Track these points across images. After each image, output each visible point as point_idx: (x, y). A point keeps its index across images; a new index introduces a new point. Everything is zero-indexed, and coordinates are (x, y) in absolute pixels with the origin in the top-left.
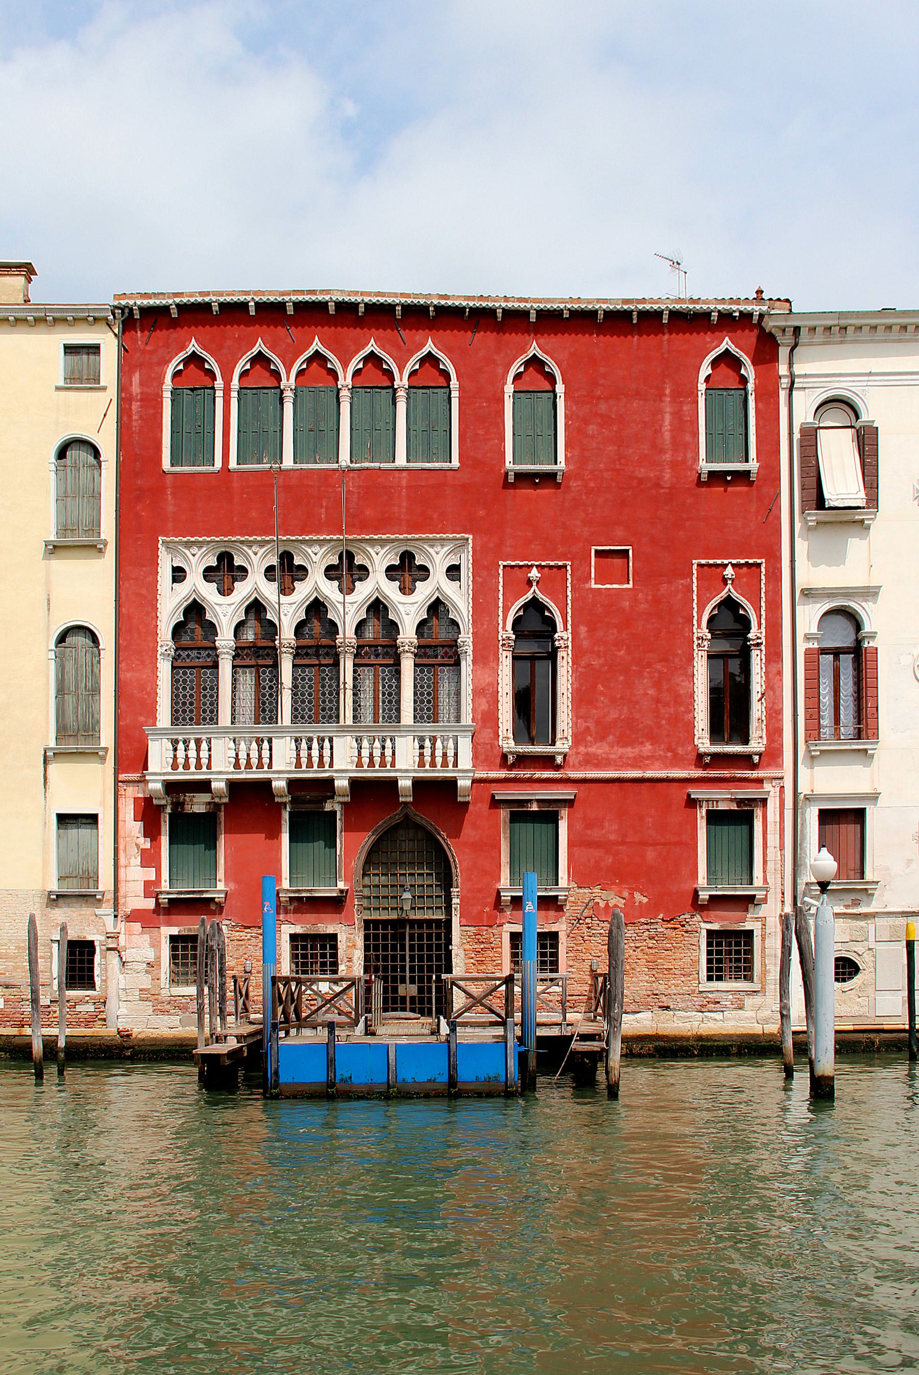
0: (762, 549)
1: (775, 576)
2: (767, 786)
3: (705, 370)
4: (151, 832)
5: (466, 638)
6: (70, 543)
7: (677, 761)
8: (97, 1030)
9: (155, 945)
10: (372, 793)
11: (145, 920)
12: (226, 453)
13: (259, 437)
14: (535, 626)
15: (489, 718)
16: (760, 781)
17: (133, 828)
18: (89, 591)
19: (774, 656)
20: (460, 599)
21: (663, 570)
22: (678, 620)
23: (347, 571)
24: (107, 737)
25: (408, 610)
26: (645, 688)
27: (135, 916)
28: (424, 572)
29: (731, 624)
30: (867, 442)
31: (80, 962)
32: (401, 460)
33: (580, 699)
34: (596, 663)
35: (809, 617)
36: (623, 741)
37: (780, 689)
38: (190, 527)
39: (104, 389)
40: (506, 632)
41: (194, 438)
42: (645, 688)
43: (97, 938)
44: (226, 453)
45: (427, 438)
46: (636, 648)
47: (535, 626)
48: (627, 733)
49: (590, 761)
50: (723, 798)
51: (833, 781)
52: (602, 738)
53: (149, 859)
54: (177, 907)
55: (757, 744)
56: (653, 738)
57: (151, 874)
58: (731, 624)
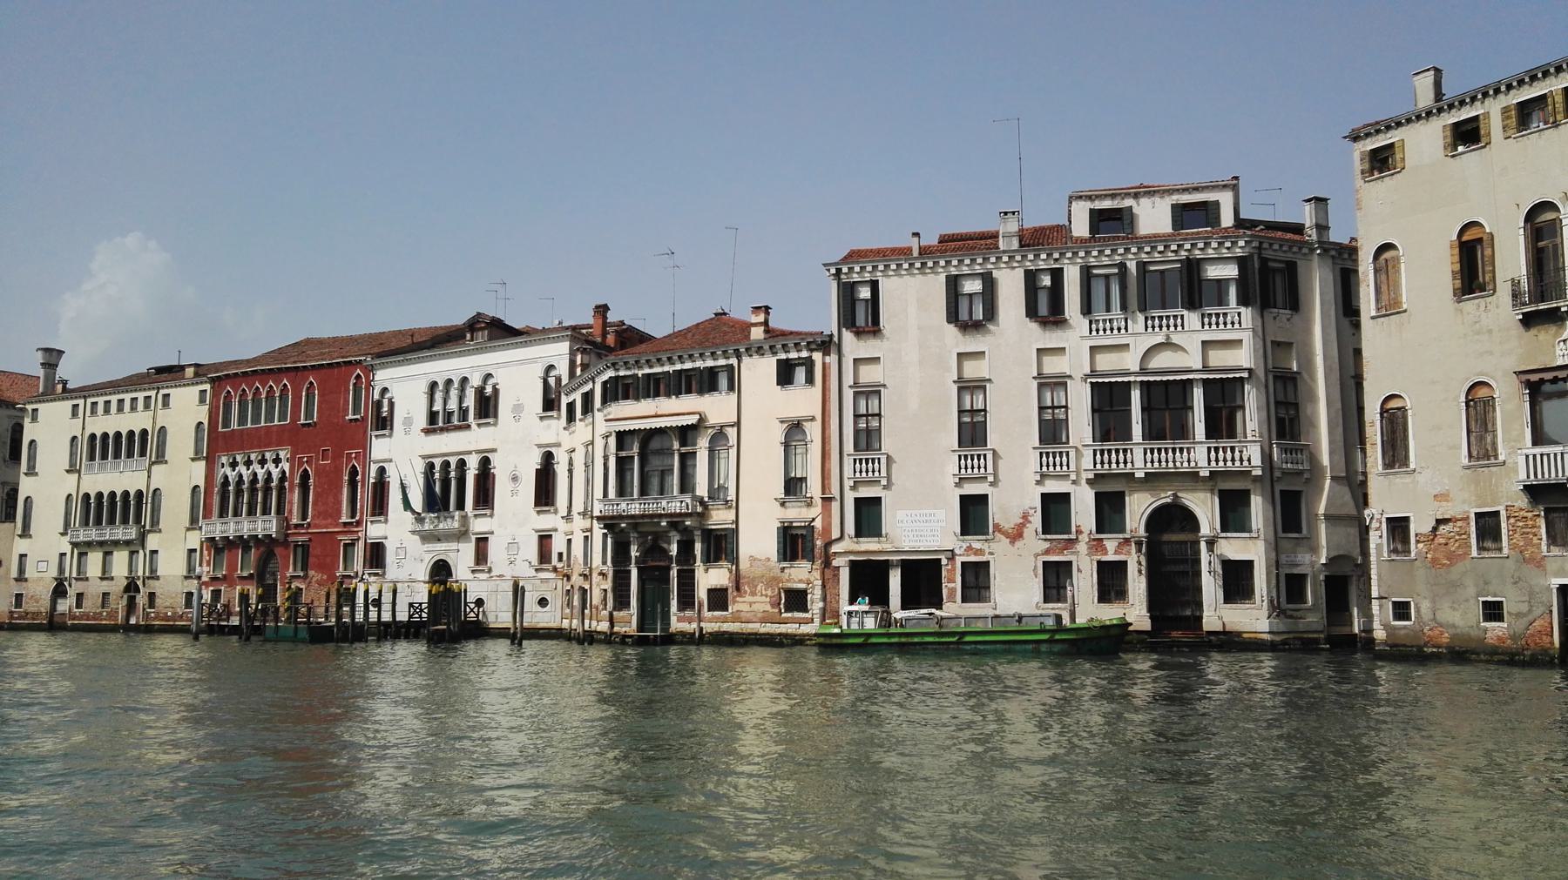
3: (353, 381)
12: (234, 425)
13: (242, 420)
15: (290, 511)
20: (286, 466)
21: (337, 456)
25: (275, 473)
26: (331, 499)
29: (354, 472)
30: (391, 404)
33: (315, 503)
35: (374, 468)
41: (226, 423)
44: (234, 425)
45: (283, 417)
49: (316, 526)
50: (346, 539)
51: (375, 531)
58: (354, 472)
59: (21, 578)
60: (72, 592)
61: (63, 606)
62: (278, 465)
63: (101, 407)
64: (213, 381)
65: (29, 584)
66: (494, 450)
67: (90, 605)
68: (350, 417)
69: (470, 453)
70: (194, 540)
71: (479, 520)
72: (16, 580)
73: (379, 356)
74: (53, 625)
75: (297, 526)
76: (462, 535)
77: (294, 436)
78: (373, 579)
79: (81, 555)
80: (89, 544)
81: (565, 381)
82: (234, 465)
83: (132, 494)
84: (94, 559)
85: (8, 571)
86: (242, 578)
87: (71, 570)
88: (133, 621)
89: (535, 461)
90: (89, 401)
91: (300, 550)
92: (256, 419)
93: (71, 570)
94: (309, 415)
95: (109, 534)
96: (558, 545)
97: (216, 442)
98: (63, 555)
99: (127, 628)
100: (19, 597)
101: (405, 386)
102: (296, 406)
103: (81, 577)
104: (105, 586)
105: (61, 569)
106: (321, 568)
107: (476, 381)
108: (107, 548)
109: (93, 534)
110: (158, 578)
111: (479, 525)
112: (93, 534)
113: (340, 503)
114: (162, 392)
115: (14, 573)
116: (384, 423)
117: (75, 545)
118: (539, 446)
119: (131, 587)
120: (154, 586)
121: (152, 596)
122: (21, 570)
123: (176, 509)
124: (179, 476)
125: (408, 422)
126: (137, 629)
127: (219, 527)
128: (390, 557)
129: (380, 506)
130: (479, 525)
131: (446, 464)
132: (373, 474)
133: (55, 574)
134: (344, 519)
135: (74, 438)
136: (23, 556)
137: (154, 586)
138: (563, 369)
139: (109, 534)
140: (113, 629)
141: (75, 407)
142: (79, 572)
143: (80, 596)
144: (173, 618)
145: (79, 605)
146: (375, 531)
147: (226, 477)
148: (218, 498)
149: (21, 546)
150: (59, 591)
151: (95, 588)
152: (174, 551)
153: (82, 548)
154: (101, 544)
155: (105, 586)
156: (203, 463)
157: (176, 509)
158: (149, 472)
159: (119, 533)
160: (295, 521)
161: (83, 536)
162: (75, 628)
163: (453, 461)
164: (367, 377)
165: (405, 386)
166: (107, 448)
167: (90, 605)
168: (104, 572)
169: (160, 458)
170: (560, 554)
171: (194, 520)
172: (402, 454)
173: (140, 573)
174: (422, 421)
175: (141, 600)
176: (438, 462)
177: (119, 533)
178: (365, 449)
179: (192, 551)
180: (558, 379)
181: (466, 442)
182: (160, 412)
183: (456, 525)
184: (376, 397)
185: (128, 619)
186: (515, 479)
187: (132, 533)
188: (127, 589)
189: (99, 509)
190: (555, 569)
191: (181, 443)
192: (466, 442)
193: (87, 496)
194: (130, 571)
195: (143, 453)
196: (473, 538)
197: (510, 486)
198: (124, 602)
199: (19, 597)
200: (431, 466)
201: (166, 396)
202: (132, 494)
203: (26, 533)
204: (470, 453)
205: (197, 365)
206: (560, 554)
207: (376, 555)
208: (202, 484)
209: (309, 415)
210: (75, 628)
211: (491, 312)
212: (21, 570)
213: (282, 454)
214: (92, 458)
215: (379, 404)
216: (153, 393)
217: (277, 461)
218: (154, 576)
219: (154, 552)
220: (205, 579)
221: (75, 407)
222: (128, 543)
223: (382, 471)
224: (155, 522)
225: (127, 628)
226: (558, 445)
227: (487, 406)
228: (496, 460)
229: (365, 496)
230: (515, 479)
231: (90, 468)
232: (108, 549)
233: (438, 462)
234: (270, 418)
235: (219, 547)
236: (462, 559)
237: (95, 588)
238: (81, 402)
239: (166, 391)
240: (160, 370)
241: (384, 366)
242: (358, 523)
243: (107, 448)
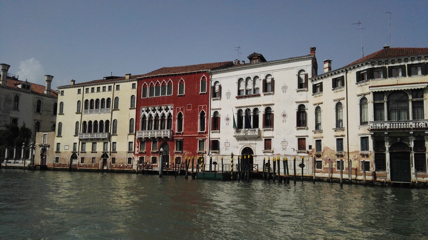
0: (207, 103)
1: (208, 107)
2: (206, 137)
3: (201, 79)
4: (138, 144)
5: (172, 118)
6: (132, 108)
7: (196, 134)
10: (160, 138)
11: (137, 155)
13: (151, 94)
14: (180, 115)
15: (174, 128)
16: (205, 136)
17: (136, 143)
18: (133, 114)
19: (208, 119)
20: (172, 112)
21: (195, 107)
22: (196, 114)
23: (160, 110)
24: (134, 133)
25: (166, 114)
26: (192, 124)
27: (136, 155)
28: (169, 109)
30: (220, 87)
31: (130, 159)
32: (166, 95)
34: (187, 120)
35: (212, 112)
36: (190, 131)
37: (209, 123)
38: (144, 105)
40: (177, 117)
41: (144, 95)
42: (192, 124)
43: (132, 157)
44: (148, 96)
45: (169, 92)
46: (192, 118)
47: (180, 115)
48: (190, 130)
50: (200, 139)
51: (214, 136)
52: (187, 131)
53: (138, 147)
54: (140, 153)
55: (205, 131)
56: (193, 130)
57: (138, 149)
58: (203, 114)
59: (58, 151)
60: (79, 157)
61: (75, 162)
62: (169, 111)
63: (90, 90)
64: (138, 80)
65: (61, 154)
66: (273, 104)
67: (86, 162)
68: (200, 92)
69: (260, 105)
70: (132, 138)
71: (266, 132)
72: (56, 152)
73: (213, 69)
74: (71, 169)
75: (177, 134)
76: (258, 138)
77: (175, 100)
78: (213, 154)
79: (82, 143)
80: (87, 140)
81: (310, 76)
82: (148, 111)
84: (89, 146)
85: (53, 149)
86: (153, 153)
87: (78, 148)
88: (105, 168)
89: (295, 108)
90: (85, 88)
91: (178, 143)
92: (157, 94)
93: (78, 148)
94: (181, 92)
95: (95, 136)
96: (310, 142)
97: (139, 102)
98: (75, 144)
99: (102, 171)
100: (57, 159)
101: (227, 81)
102: (175, 89)
103: (83, 151)
104: (93, 155)
105: (74, 149)
106: (188, 150)
107: (262, 77)
108: (94, 141)
109: (89, 136)
110: (116, 152)
111: (266, 134)
112: (89, 136)
113: (197, 125)
114: (116, 84)
115: (55, 150)
116: (217, 95)
117: (80, 140)
118: (297, 102)
119: (105, 156)
120: (114, 155)
121: (114, 159)
122: (58, 149)
123: (123, 127)
124: (125, 115)
125: (228, 94)
126: (107, 171)
127: (144, 134)
128: (222, 146)
130: (266, 134)
131: (248, 110)
132: (212, 114)
133: (72, 150)
134: (199, 131)
135: (79, 102)
136: (58, 144)
138: (309, 71)
139: (95, 136)
140: (97, 171)
141: (79, 90)
142: (82, 150)
143: (83, 159)
144: (123, 167)
145: (82, 162)
147: (144, 115)
148: (139, 124)
149: (58, 140)
150: (74, 156)
151: (89, 155)
152: (123, 143)
153: (83, 142)
154: (92, 140)
155: (93, 155)
156: (135, 111)
157: (123, 127)
158: (112, 114)
159: (101, 136)
160: (176, 132)
161: (84, 136)
162: (81, 171)
163: (252, 109)
164: (208, 78)
165: (227, 81)
166: (92, 105)
167: (86, 162)
168: (93, 150)
169: (116, 108)
170: (310, 147)
171: (131, 131)
172: (227, 107)
173: (109, 150)
174: (235, 93)
175: (109, 160)
176: (244, 110)
177: (101, 136)
178: (208, 105)
179: (130, 143)
180: (306, 76)
181: (261, 101)
182: (115, 92)
183: (257, 134)
184: (213, 85)
185: (103, 167)
186: (284, 116)
187: (106, 136)
188: (103, 156)
189: (89, 127)
190: (308, 152)
191: (125, 102)
192: (261, 101)
193: (85, 122)
194: (104, 150)
195: (108, 106)
196: (263, 139)
197: (282, 118)
198: (102, 161)
199: (57, 159)
200: (240, 112)
201: (118, 86)
203: (59, 135)
204: (260, 105)
205: (130, 74)
206: (310, 147)
207: (215, 145)
209: (181, 92)
210: (81, 171)
211: (258, 52)
212: (58, 149)
213: (169, 107)
214: (86, 108)
215: (214, 88)
216: (112, 85)
217: (167, 109)
218: (114, 151)
219: (114, 143)
220: (136, 153)
221: (79, 90)
222: (103, 139)
223: (216, 113)
224: (115, 132)
225: (102, 171)
226: (307, 102)
227: (269, 87)
228: (273, 108)
229: (209, 123)
230: (284, 116)
231: (86, 112)
232: (94, 141)
233: (244, 110)
234: (164, 93)
235: (142, 141)
236: (258, 148)
237: (89, 155)
238: (82, 88)
239: (118, 84)
240: (108, 78)
241: (216, 73)
242: (206, 133)
243: (92, 105)
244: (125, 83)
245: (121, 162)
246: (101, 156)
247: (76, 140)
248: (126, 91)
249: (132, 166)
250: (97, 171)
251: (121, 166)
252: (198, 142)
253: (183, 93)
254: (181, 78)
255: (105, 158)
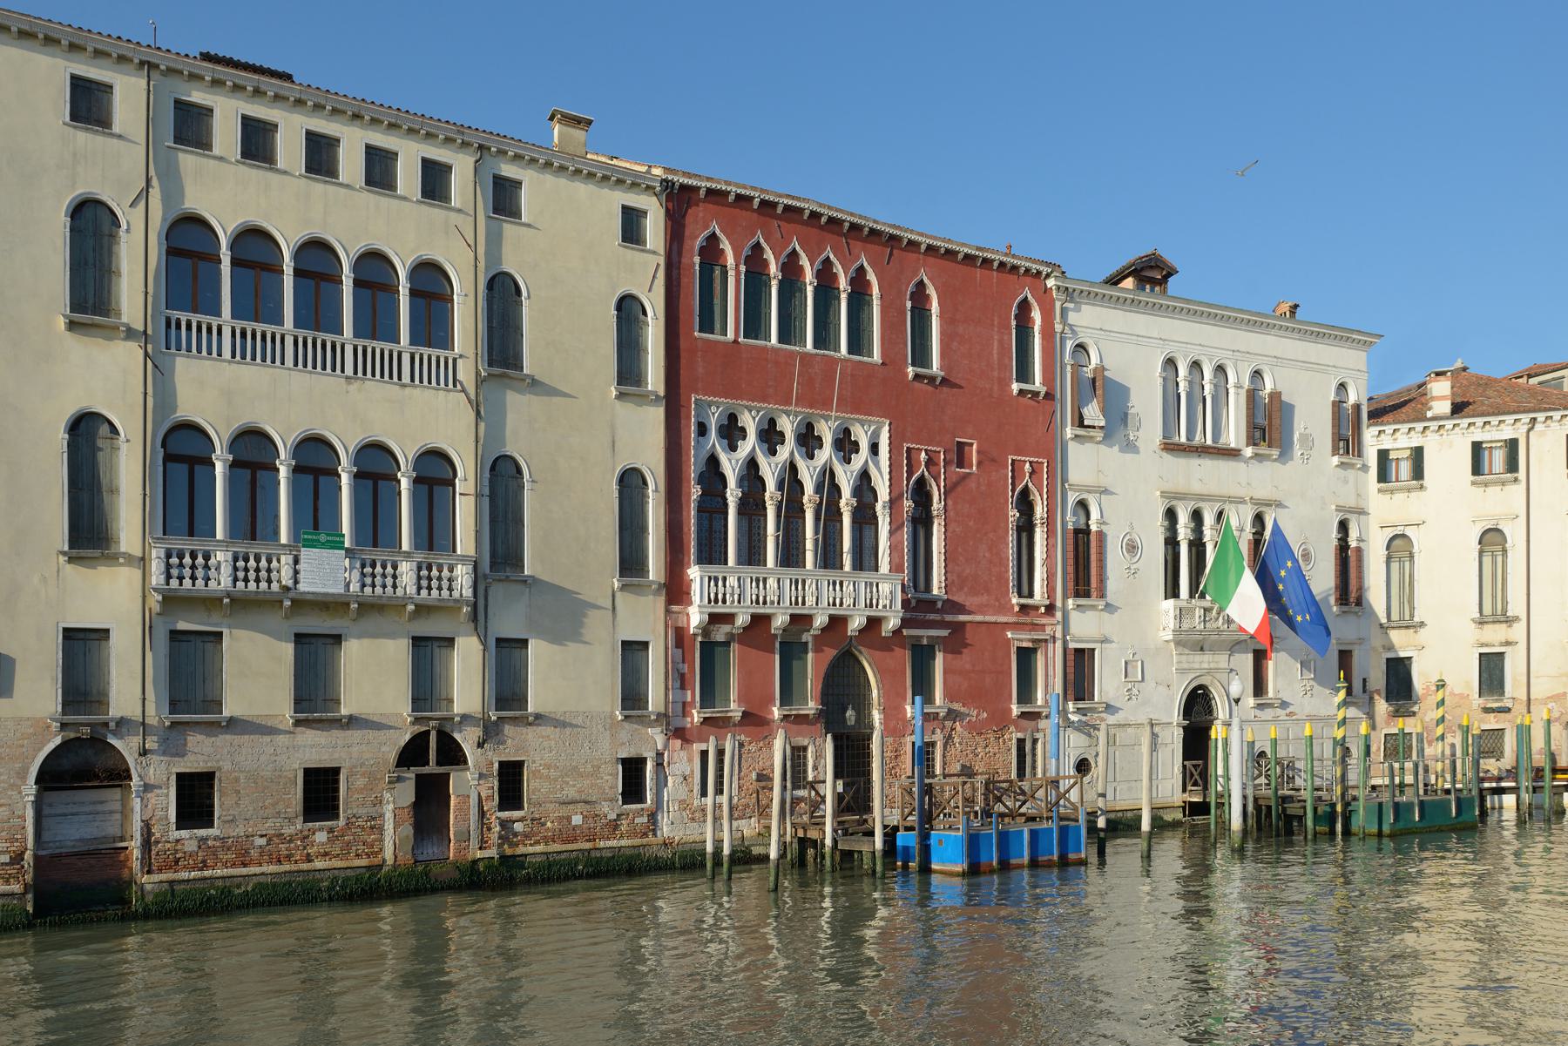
8: (650, 839)
9: (690, 760)
18: (642, 437)
39: (654, 253)
51: (1084, 624)
64: (679, 199)
83: (405, 455)
104: (316, 748)
120: (519, 743)
121: (510, 779)
129: (1084, 574)
137: (519, 743)
140: (366, 890)
146: (1084, 624)
175: (470, 787)
188: (412, 754)
202: (405, 455)
208: (653, 465)
223: (1083, 505)
242: (1050, 609)
244: (562, 182)
245: (571, 793)
246: (392, 756)
247: (114, 598)
248: (580, 257)
249: (653, 816)
250: (366, 890)
251: (577, 820)
252: (1014, 657)
253: (928, 365)
254: (916, 272)
255: (432, 768)
